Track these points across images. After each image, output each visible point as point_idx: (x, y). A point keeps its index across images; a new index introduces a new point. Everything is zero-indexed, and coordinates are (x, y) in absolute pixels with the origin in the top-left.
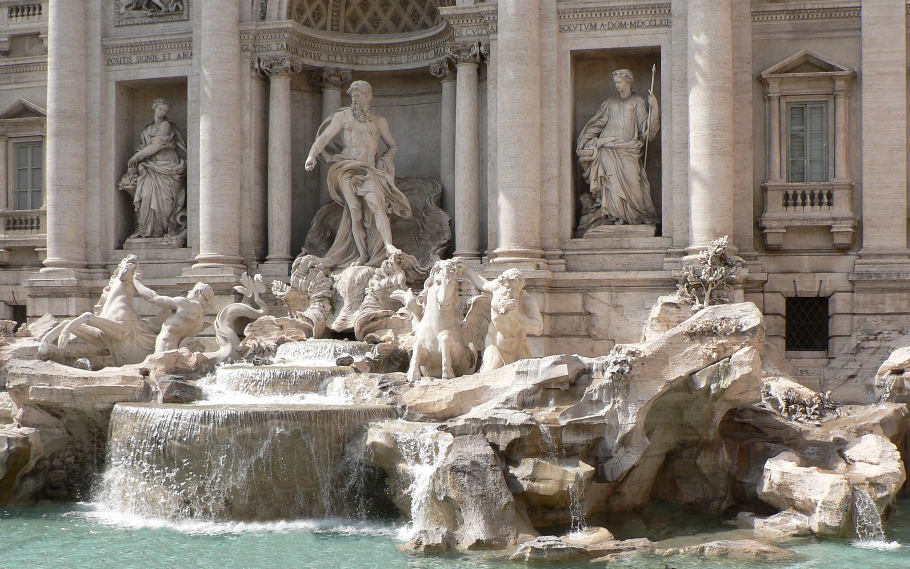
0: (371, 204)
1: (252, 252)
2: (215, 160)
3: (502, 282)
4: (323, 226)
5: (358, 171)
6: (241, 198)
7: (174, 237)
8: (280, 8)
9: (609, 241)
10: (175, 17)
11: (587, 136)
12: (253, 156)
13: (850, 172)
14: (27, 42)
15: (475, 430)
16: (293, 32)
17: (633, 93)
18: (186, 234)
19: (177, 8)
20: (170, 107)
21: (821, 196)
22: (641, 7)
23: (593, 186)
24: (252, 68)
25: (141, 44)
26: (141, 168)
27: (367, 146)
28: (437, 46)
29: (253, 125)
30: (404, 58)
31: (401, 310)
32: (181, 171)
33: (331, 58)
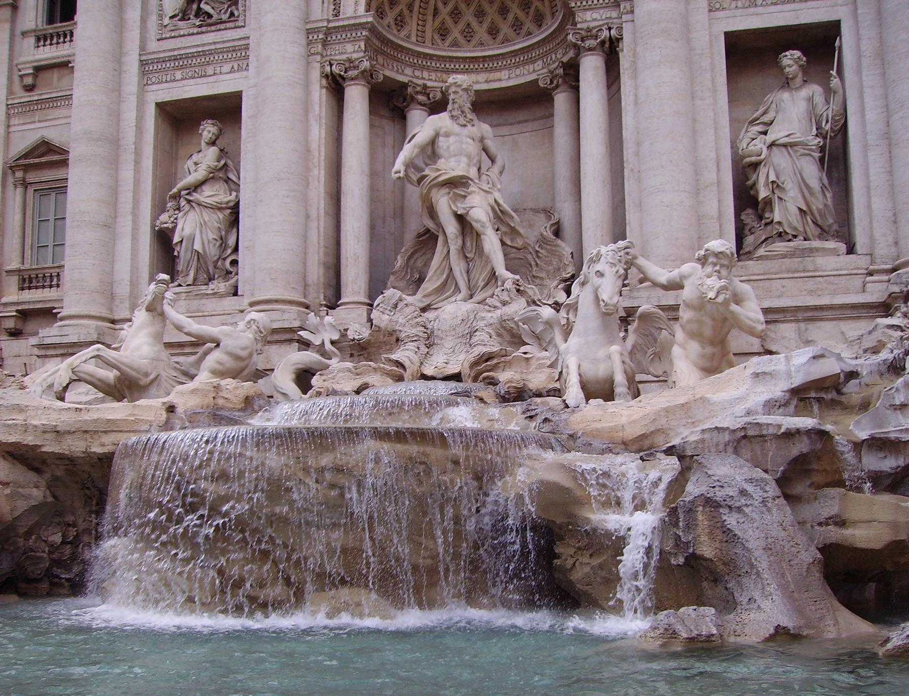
0: (477, 221)
1: (318, 297)
5: (456, 184)
11: (750, 135)
12: (323, 179)
14: (56, 74)
15: (721, 447)
16: (373, 30)
18: (237, 281)
19: (232, 14)
20: (220, 130)
23: (763, 194)
25: (187, 56)
26: (183, 203)
27: (469, 157)
28: (546, 54)
29: (323, 141)
30: (504, 74)
31: (523, 349)
32: (232, 204)
33: (417, 73)
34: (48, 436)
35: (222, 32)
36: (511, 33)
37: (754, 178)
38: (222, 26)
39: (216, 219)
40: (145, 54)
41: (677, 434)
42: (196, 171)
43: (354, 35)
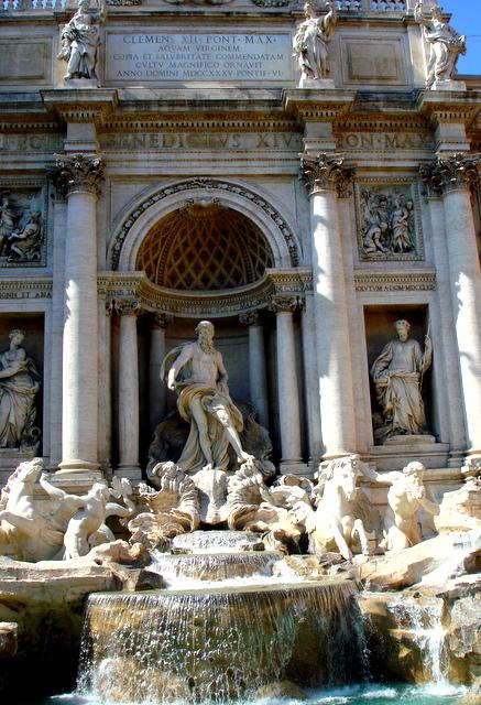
2: (81, 381)
3: (411, 473)
4: (161, 438)
6: (99, 414)
8: (130, 262)
9: (404, 448)
17: (408, 338)
19: (36, 257)
20: (25, 337)
22: (414, 276)
23: (389, 405)
24: (107, 308)
27: (211, 373)
28: (243, 301)
30: (213, 309)
31: (263, 505)
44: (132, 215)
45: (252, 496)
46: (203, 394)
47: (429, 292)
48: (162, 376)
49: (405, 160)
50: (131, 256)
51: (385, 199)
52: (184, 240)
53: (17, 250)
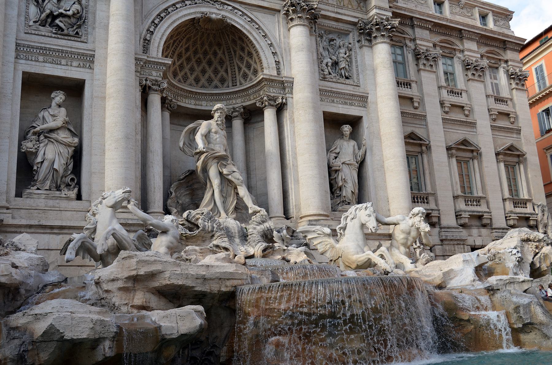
0: (238, 179)
7: (72, 192)
10: (76, 39)
13: (432, 190)
21: (423, 199)
23: (340, 184)
25: (50, 49)
26: (42, 137)
28: (230, 99)
30: (204, 103)
32: (76, 145)
34: (198, 281)
35: (71, 42)
36: (207, 85)
37: (336, 176)
38: (73, 38)
39: (67, 152)
40: (20, 40)
41: (449, 283)
42: (54, 120)
43: (158, 67)
44: (159, 15)
45: (267, 237)
46: (221, 159)
47: (362, 109)
48: (181, 144)
49: (348, 15)
50: (158, 46)
51: (333, 40)
52: (187, 46)
53: (61, 25)
